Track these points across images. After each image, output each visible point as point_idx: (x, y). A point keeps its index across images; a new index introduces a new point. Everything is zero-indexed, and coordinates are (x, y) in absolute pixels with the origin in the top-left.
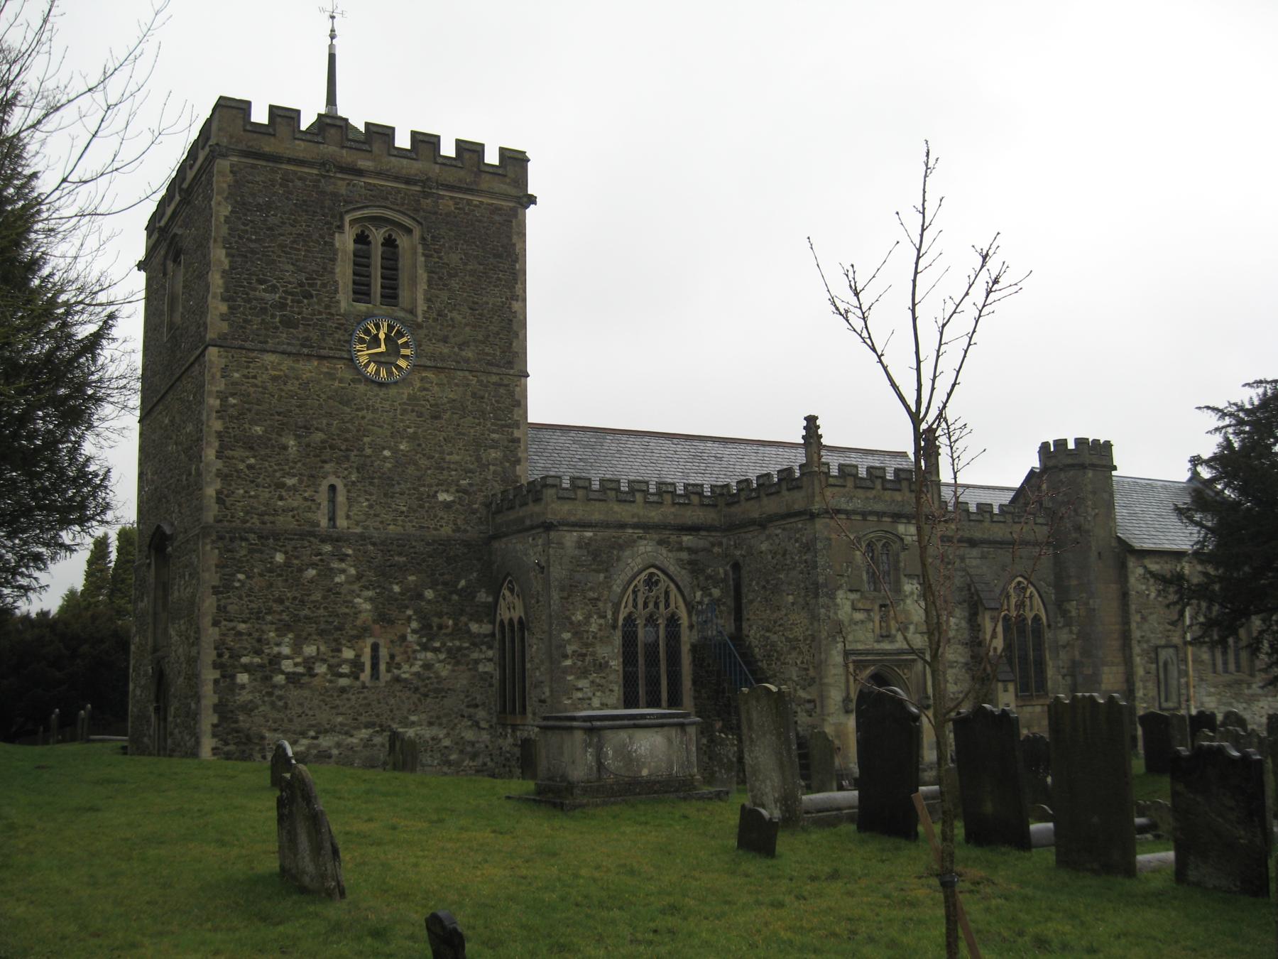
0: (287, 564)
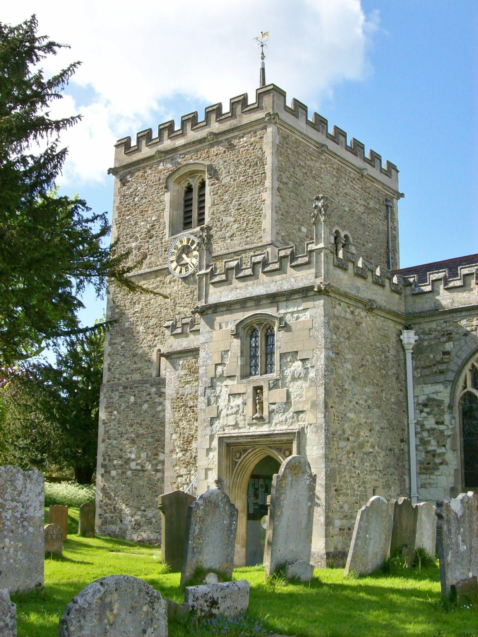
0: (135, 403)
